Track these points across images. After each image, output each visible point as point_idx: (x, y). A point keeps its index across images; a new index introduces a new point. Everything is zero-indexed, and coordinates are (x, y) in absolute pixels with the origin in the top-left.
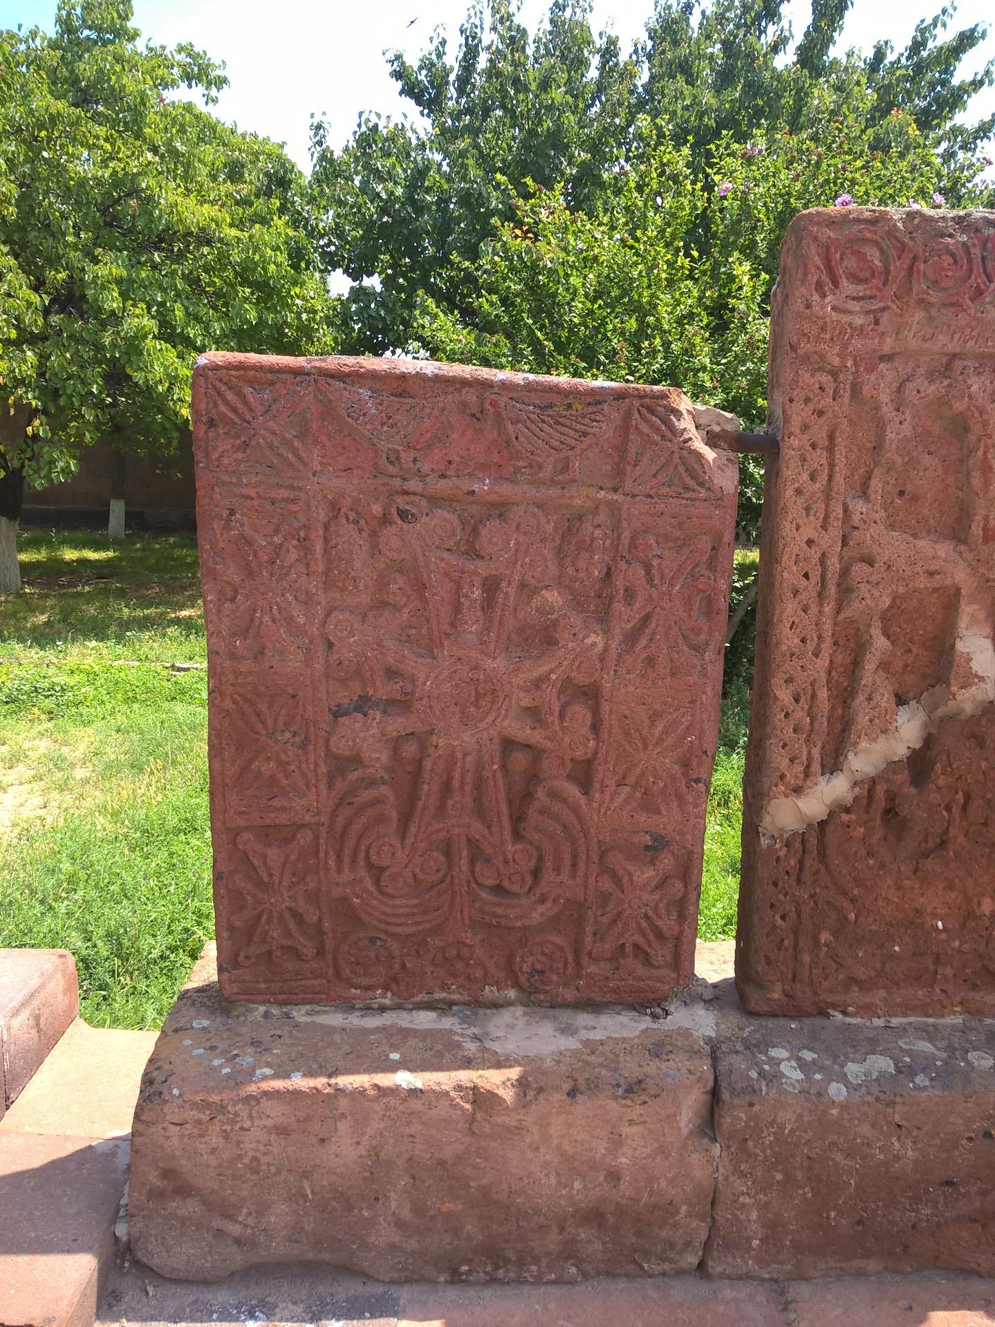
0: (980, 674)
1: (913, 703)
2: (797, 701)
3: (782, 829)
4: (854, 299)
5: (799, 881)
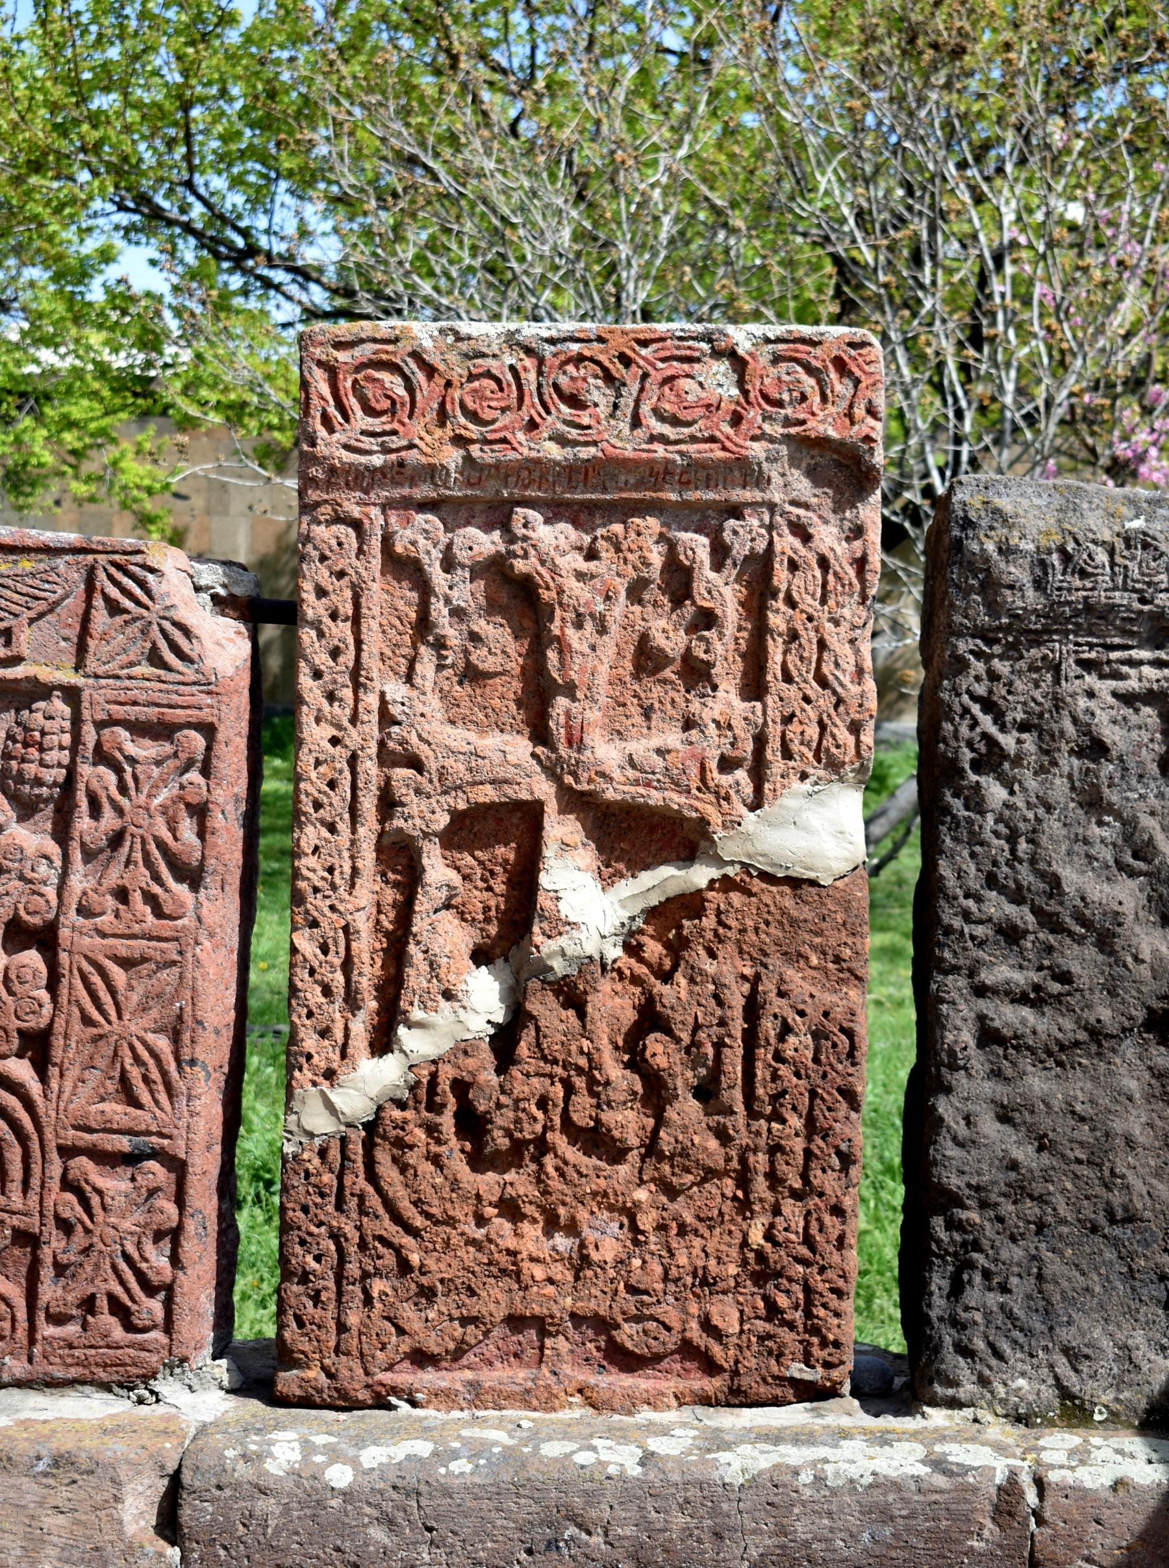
1: (500, 962)
5: (339, 1206)
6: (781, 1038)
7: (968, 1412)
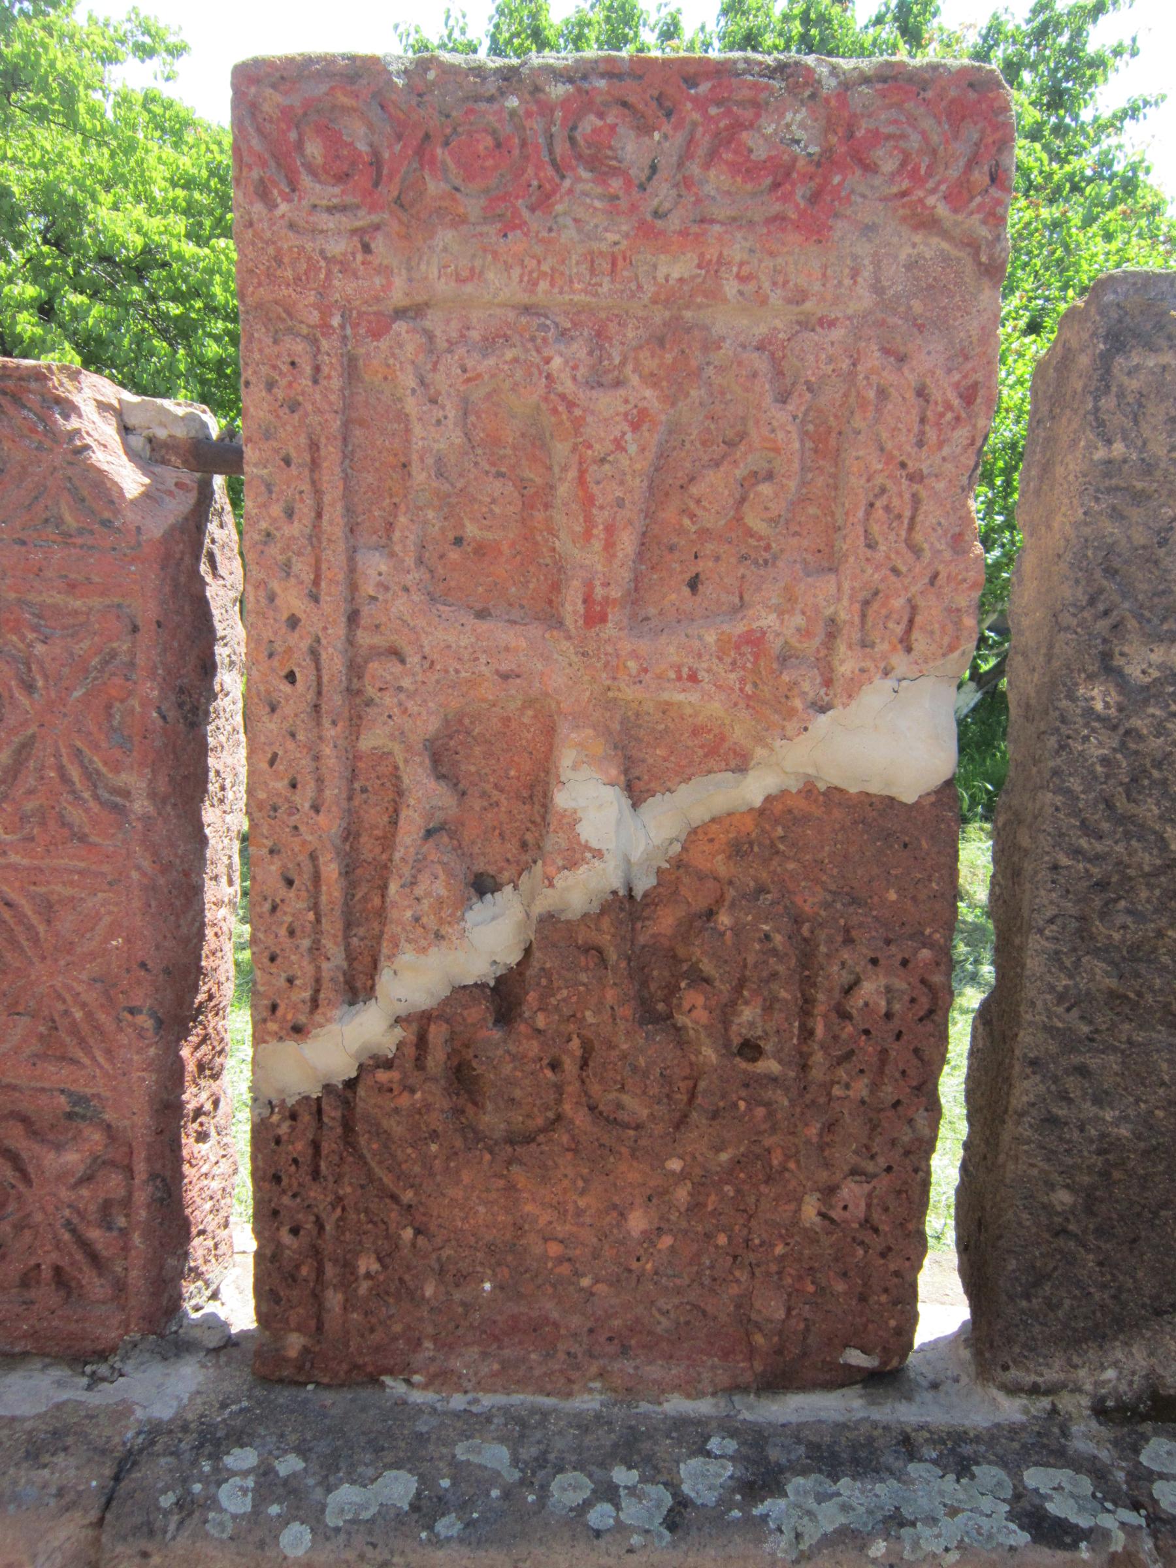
0: (594, 844)
2: (290, 883)
3: (281, 1091)
4: (330, 210)
5: (316, 1174)
6: (849, 990)
7: (1045, 1403)
